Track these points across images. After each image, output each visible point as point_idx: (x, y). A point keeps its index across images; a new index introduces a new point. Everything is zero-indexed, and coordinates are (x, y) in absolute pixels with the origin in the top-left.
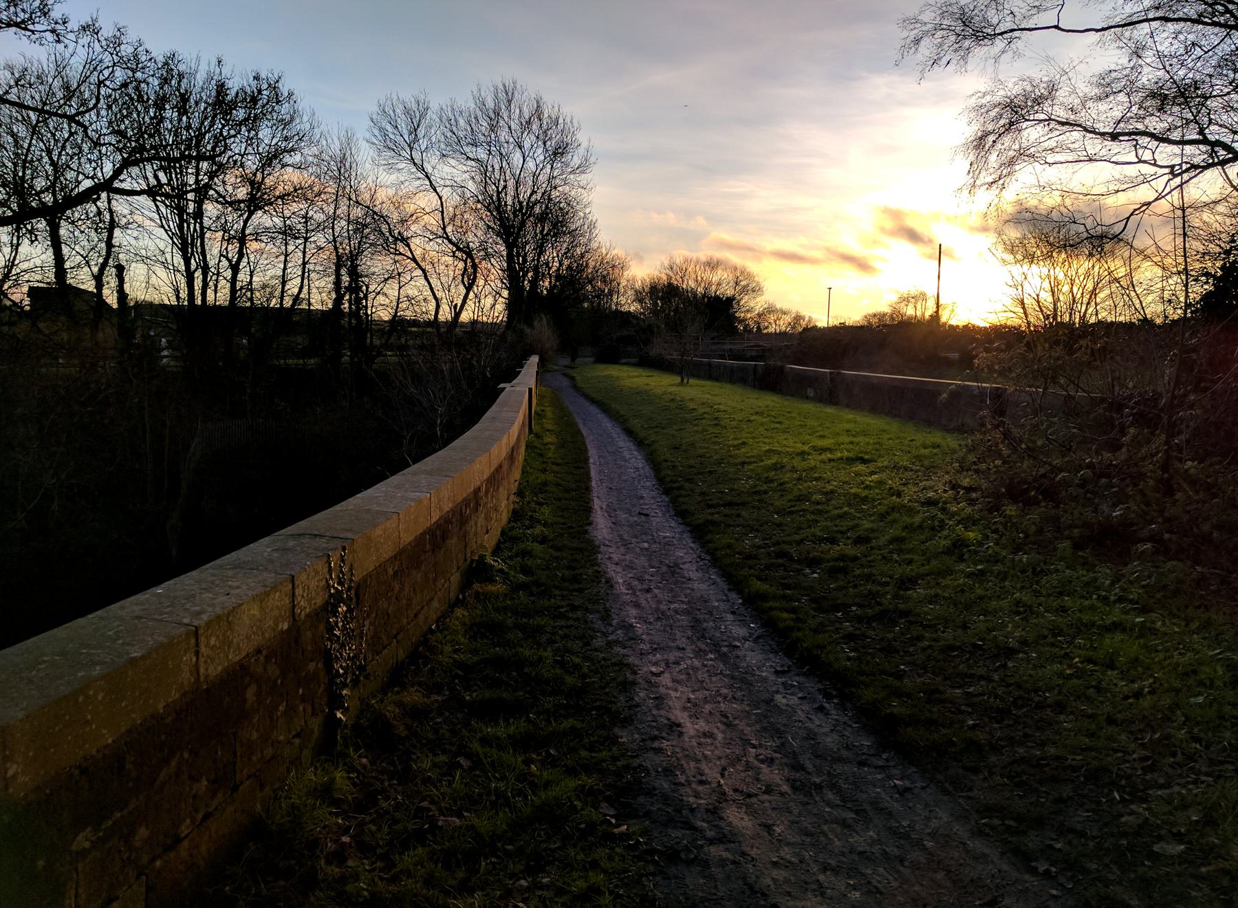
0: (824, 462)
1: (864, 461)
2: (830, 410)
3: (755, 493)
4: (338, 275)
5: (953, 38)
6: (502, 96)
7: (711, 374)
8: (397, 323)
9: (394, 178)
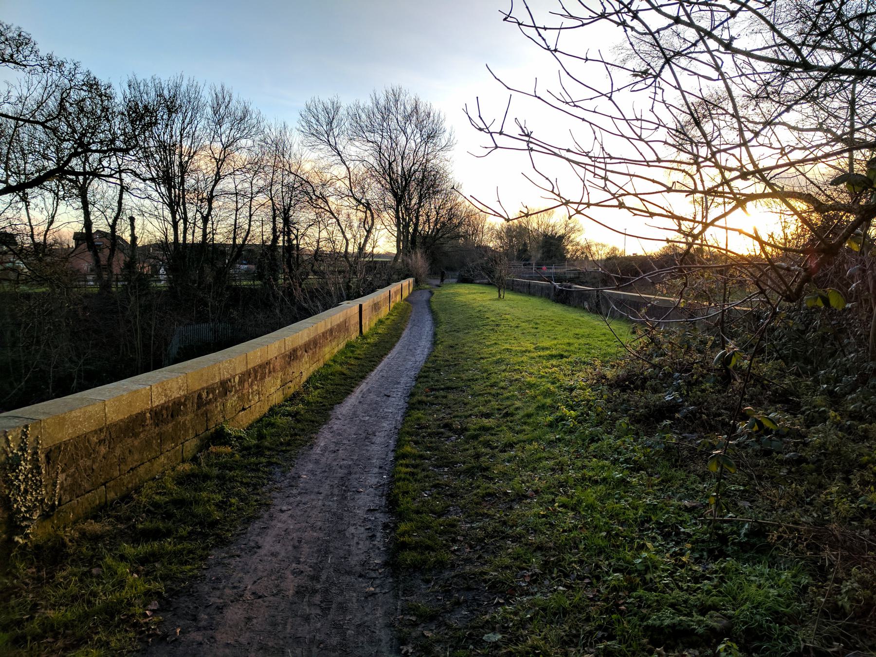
3: (469, 380)
6: (391, 97)
7: (529, 291)
8: (318, 255)
9: (314, 155)
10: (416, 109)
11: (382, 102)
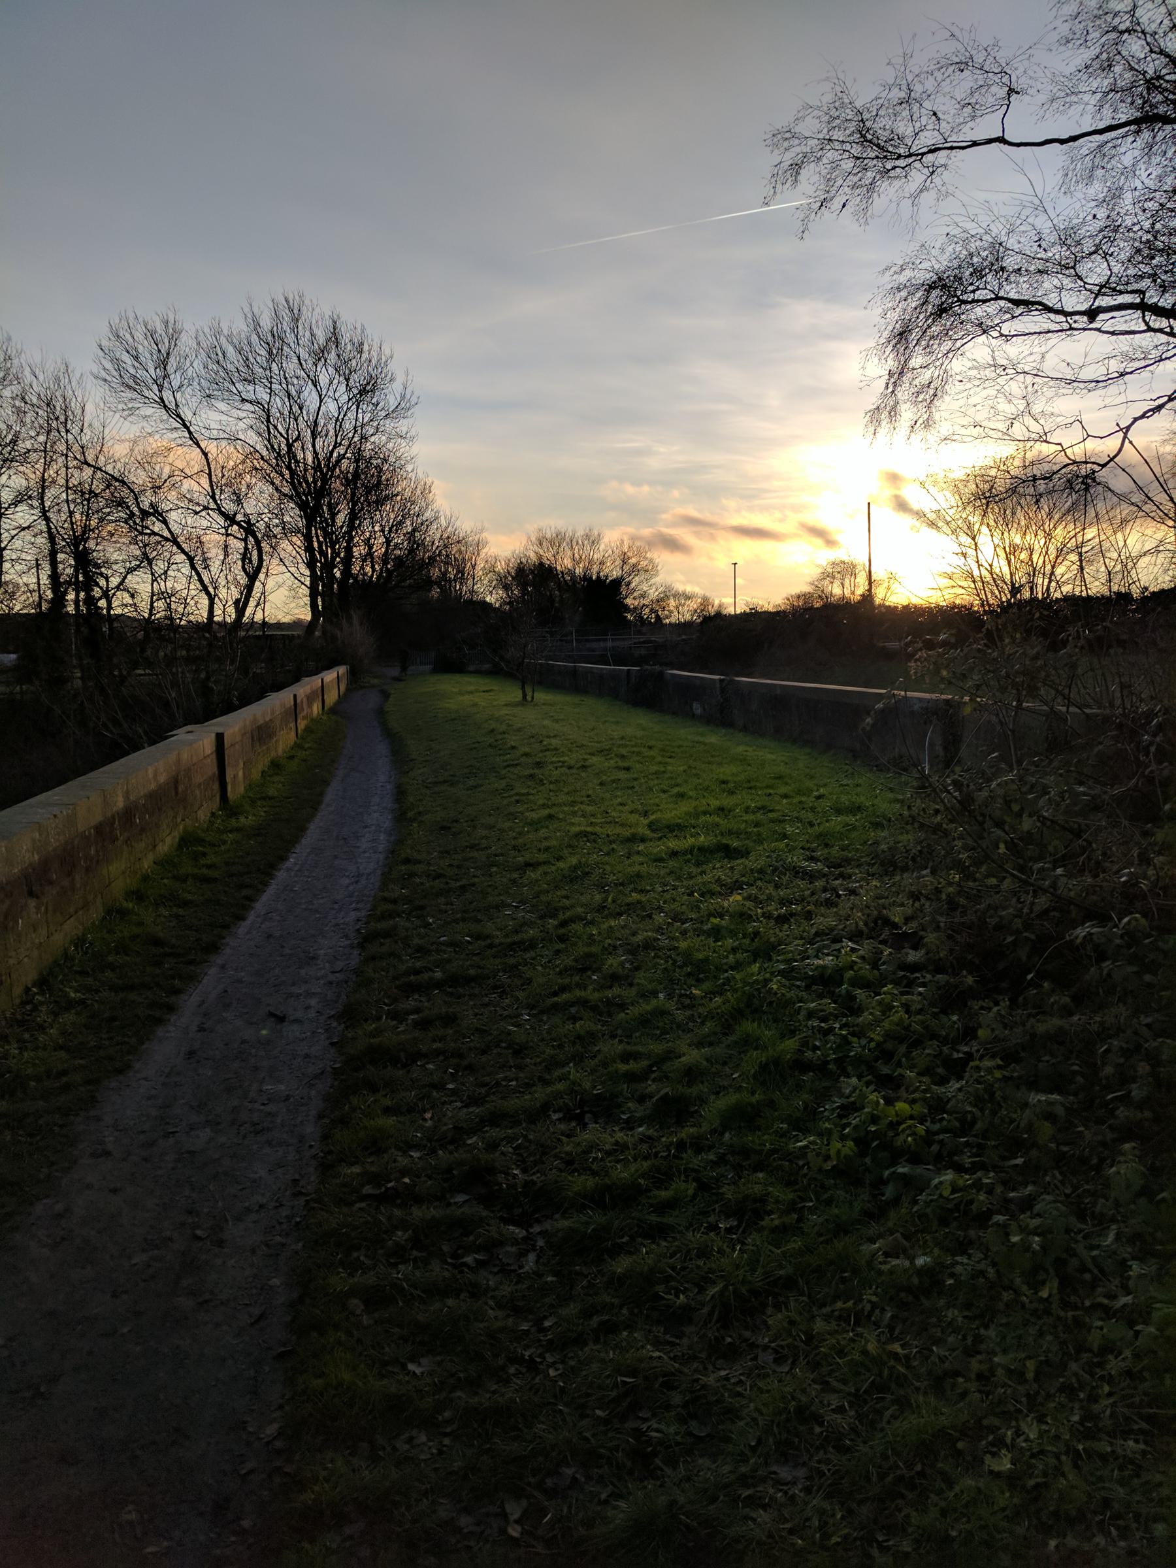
0: (661, 860)
1: (729, 853)
2: (714, 738)
3: (513, 946)
4: (54, 563)
5: (848, 165)
6: (285, 314)
7: (575, 684)
9: (131, 429)
10: (334, 338)
11: (266, 322)
